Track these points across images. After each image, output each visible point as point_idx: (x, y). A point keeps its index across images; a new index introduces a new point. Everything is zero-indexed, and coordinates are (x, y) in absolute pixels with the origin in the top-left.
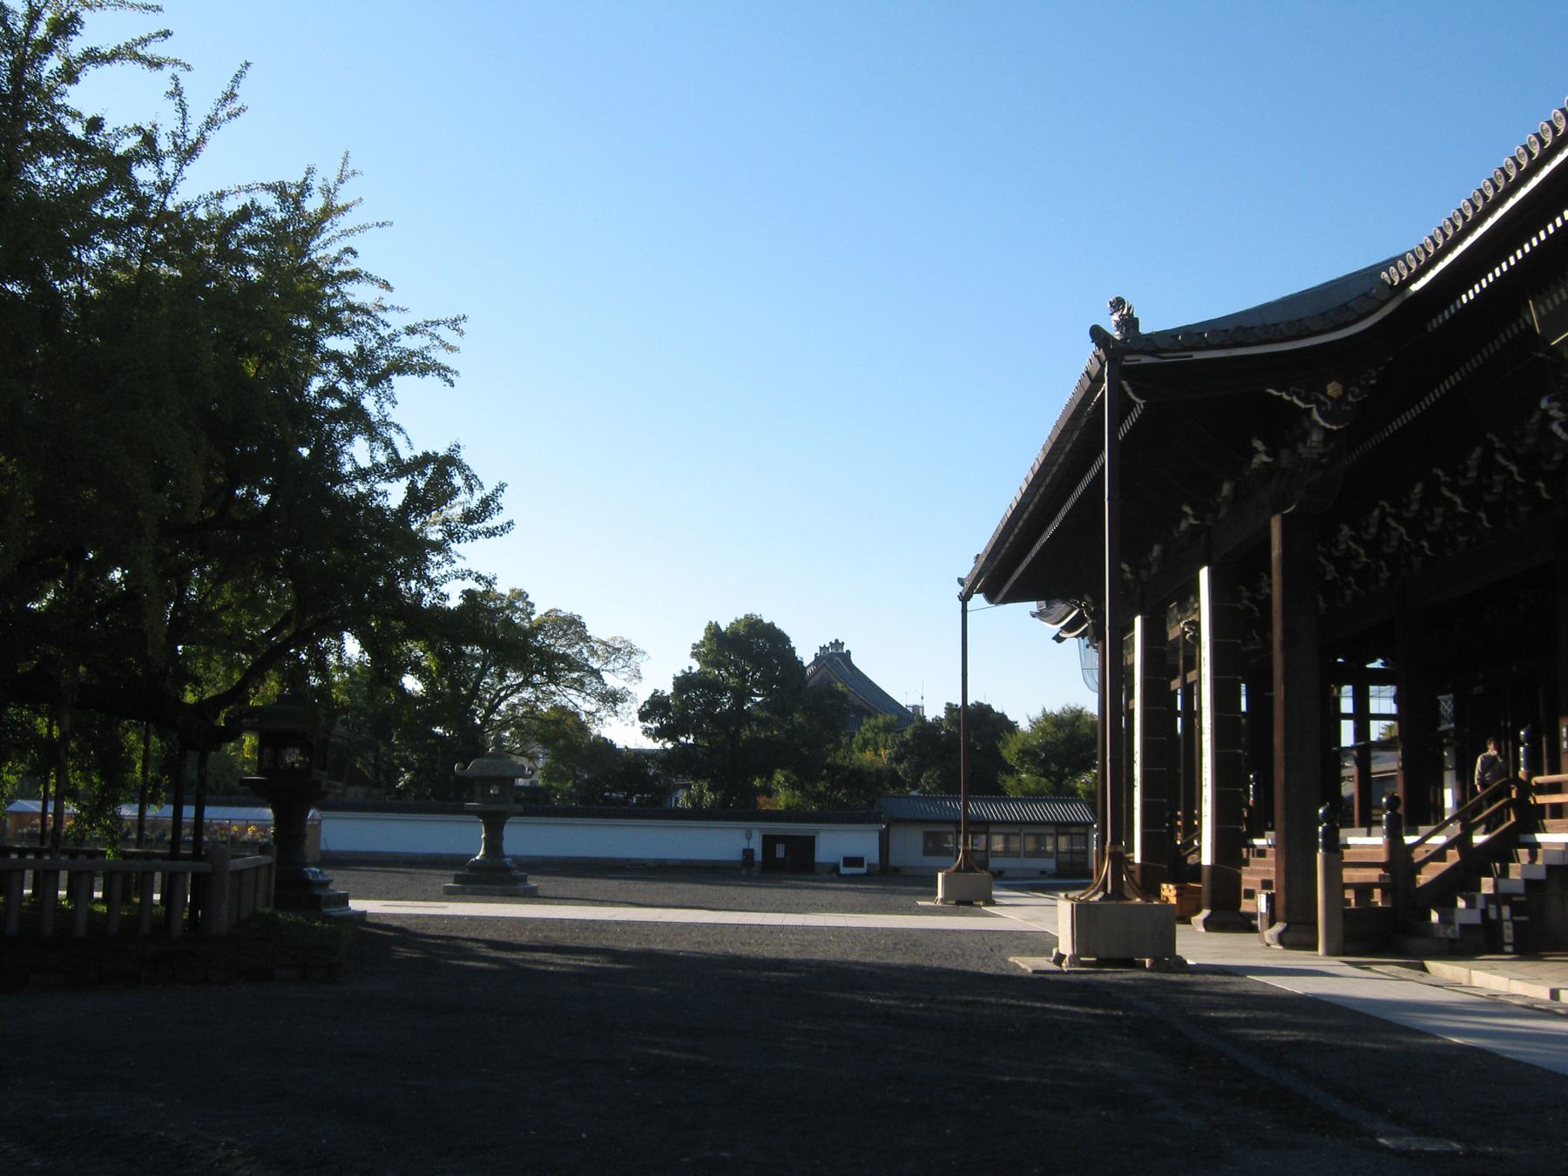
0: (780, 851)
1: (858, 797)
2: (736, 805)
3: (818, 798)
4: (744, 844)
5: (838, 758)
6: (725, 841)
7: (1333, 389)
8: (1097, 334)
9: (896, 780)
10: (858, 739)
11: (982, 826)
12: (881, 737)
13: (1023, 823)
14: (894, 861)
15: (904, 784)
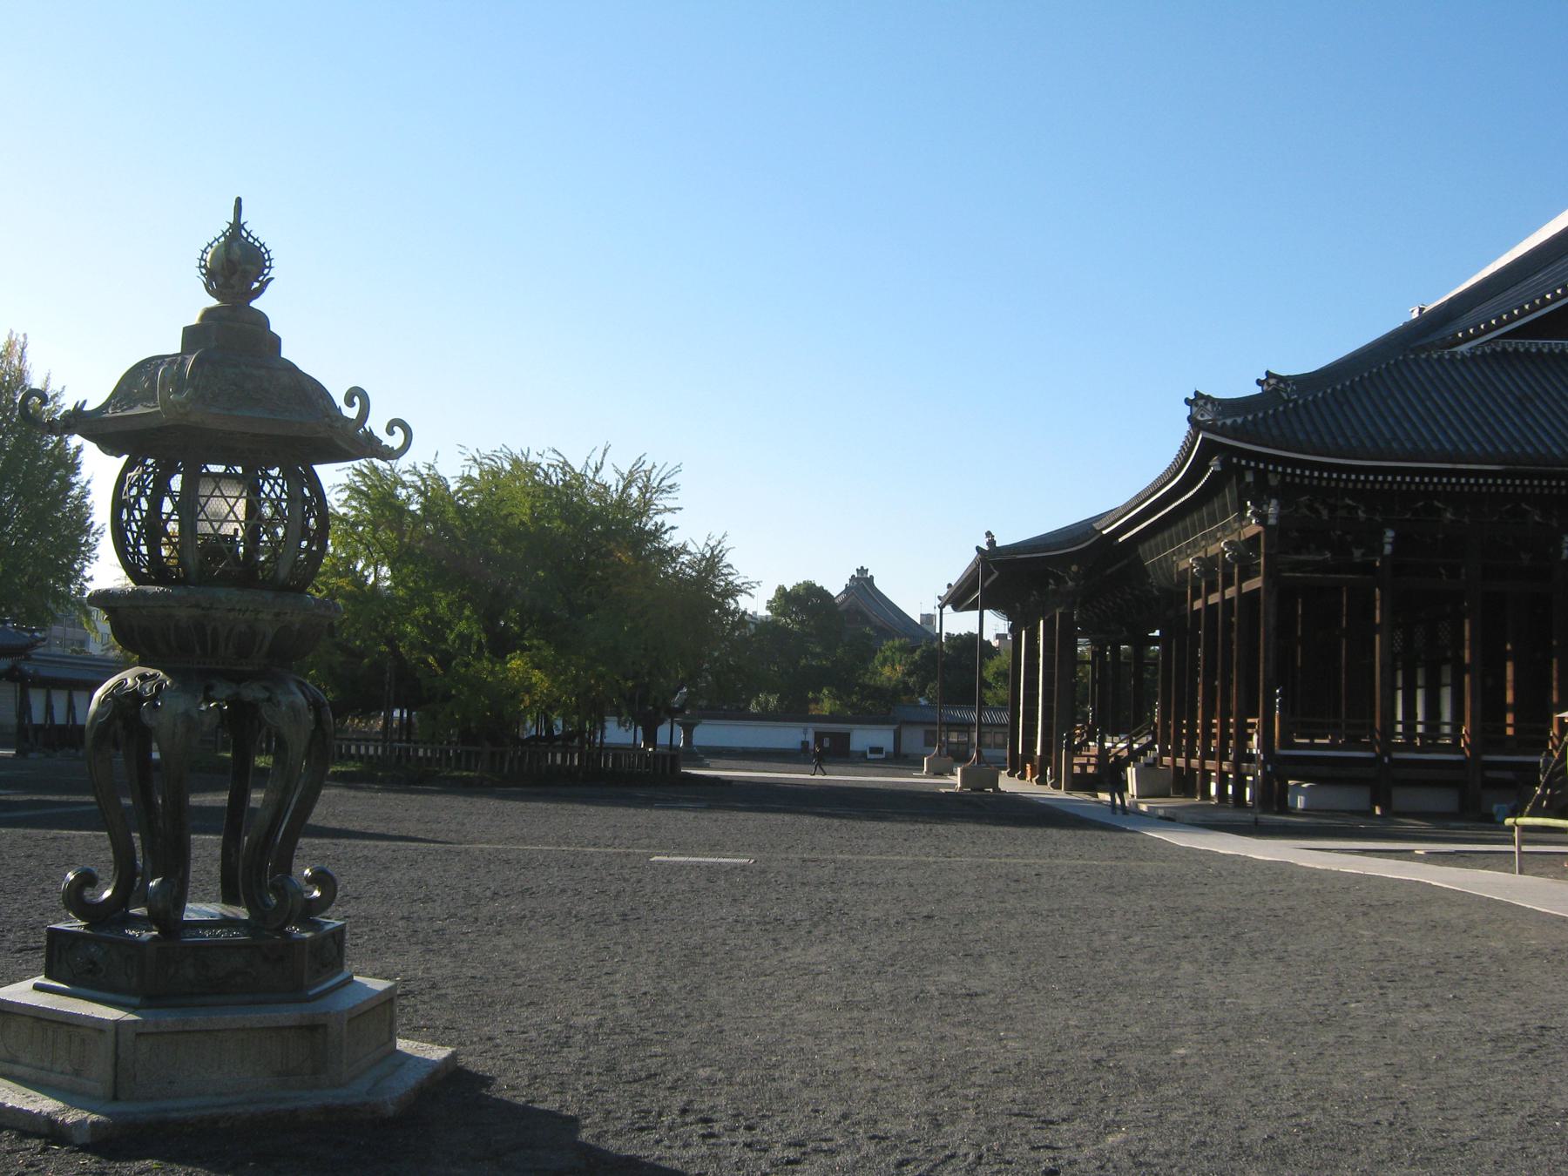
0: (826, 744)
1: (883, 705)
2: (793, 711)
3: (852, 706)
4: (801, 738)
5: (866, 679)
6: (790, 736)
7: (1074, 568)
8: (978, 548)
9: (907, 689)
10: (879, 656)
11: (965, 727)
12: (898, 655)
13: (993, 725)
14: (905, 749)
15: (913, 692)
